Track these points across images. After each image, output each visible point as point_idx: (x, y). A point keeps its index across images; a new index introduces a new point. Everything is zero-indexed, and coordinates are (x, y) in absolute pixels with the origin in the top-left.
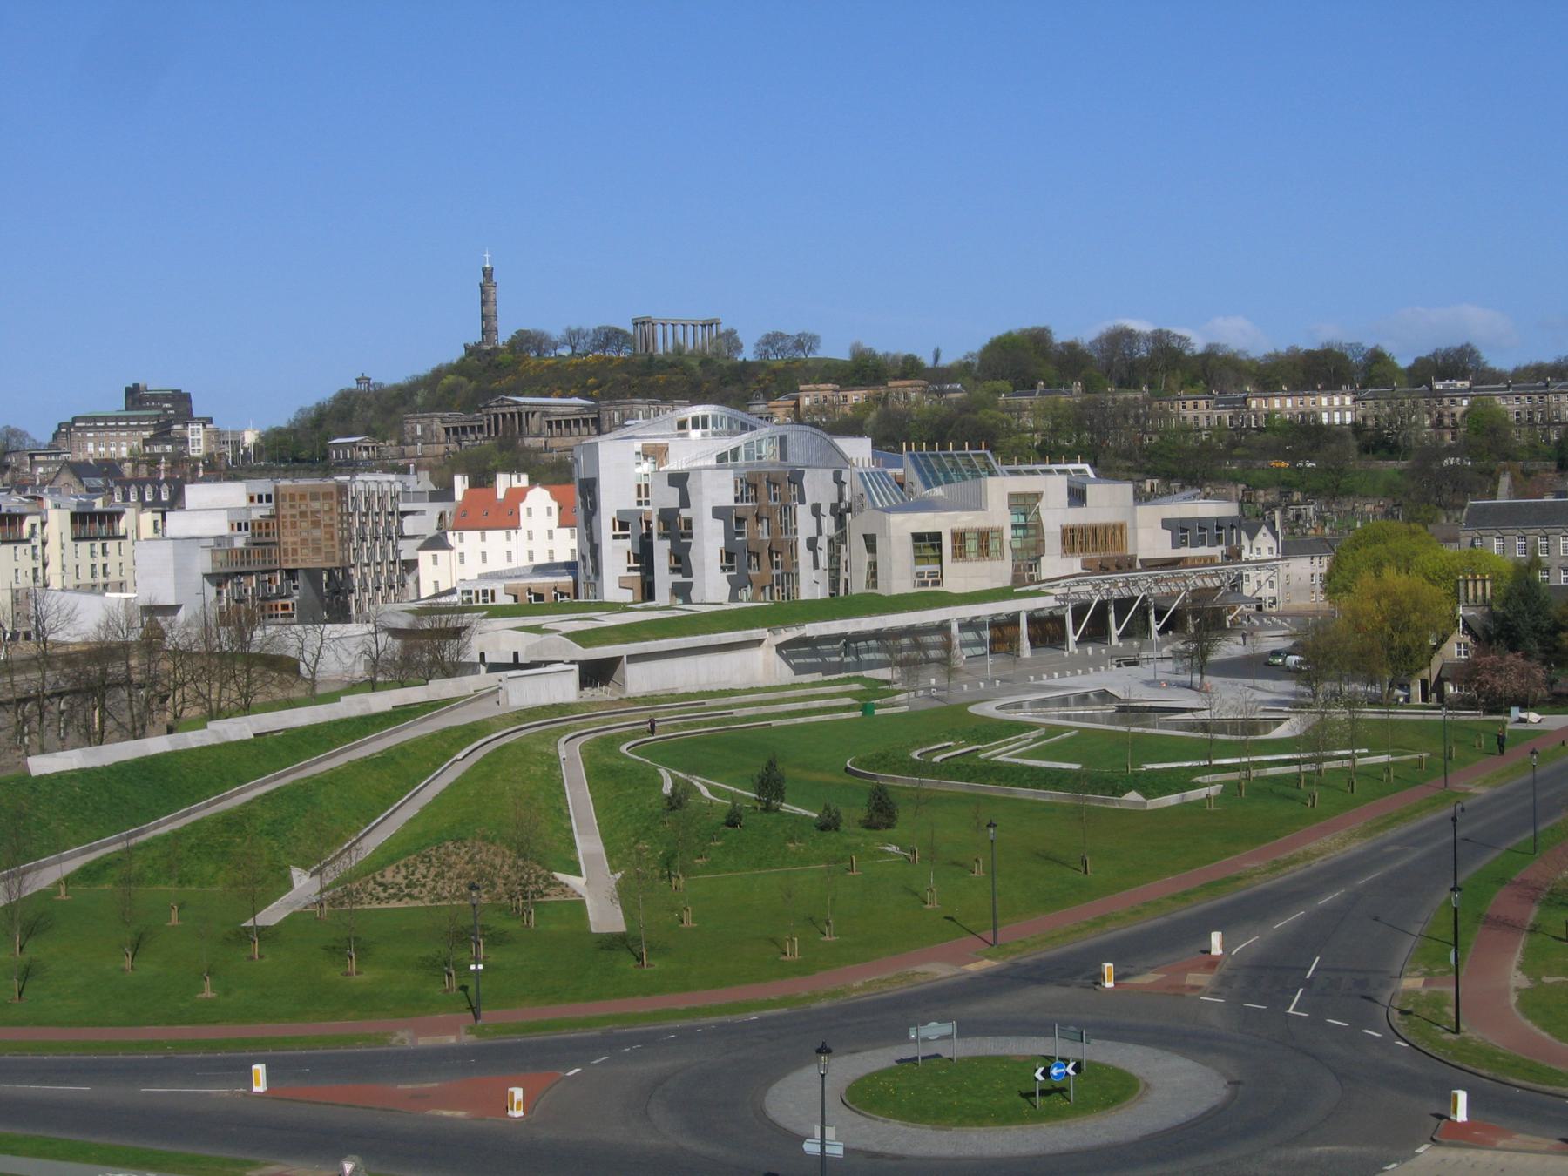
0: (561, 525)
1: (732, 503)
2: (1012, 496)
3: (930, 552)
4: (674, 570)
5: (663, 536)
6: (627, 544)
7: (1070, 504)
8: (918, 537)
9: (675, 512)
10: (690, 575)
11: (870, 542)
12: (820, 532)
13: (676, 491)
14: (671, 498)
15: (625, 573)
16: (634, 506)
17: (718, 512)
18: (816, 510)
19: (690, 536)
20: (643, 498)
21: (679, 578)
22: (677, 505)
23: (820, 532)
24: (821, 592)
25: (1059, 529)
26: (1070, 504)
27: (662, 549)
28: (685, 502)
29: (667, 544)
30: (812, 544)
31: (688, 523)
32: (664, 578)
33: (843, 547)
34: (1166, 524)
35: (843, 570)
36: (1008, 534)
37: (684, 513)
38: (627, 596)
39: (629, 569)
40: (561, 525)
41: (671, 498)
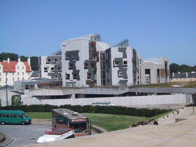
0: (3, 72)
4: (119, 77)
5: (114, 66)
6: (87, 70)
9: (121, 59)
10: (127, 78)
11: (148, 71)
13: (122, 53)
14: (120, 55)
15: (87, 79)
16: (89, 60)
19: (127, 66)
20: (90, 57)
21: (122, 79)
24: (156, 82)
27: (115, 71)
28: (125, 56)
29: (118, 69)
31: (126, 63)
32: (115, 80)
33: (137, 73)
35: (137, 79)
37: (124, 60)
38: (88, 86)
39: (88, 78)
40: (3, 72)
41: (120, 55)
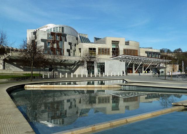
1: (47, 39)
2: (112, 41)
3: (93, 52)
7: (126, 45)
8: (90, 49)
12: (71, 48)
17: (42, 40)
18: (70, 44)
22: (34, 39)
23: (71, 48)
25: (123, 50)
26: (126, 45)
30: (68, 51)
31: (36, 42)
34: (146, 52)
36: (111, 50)
